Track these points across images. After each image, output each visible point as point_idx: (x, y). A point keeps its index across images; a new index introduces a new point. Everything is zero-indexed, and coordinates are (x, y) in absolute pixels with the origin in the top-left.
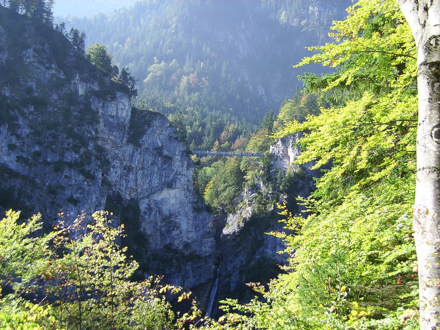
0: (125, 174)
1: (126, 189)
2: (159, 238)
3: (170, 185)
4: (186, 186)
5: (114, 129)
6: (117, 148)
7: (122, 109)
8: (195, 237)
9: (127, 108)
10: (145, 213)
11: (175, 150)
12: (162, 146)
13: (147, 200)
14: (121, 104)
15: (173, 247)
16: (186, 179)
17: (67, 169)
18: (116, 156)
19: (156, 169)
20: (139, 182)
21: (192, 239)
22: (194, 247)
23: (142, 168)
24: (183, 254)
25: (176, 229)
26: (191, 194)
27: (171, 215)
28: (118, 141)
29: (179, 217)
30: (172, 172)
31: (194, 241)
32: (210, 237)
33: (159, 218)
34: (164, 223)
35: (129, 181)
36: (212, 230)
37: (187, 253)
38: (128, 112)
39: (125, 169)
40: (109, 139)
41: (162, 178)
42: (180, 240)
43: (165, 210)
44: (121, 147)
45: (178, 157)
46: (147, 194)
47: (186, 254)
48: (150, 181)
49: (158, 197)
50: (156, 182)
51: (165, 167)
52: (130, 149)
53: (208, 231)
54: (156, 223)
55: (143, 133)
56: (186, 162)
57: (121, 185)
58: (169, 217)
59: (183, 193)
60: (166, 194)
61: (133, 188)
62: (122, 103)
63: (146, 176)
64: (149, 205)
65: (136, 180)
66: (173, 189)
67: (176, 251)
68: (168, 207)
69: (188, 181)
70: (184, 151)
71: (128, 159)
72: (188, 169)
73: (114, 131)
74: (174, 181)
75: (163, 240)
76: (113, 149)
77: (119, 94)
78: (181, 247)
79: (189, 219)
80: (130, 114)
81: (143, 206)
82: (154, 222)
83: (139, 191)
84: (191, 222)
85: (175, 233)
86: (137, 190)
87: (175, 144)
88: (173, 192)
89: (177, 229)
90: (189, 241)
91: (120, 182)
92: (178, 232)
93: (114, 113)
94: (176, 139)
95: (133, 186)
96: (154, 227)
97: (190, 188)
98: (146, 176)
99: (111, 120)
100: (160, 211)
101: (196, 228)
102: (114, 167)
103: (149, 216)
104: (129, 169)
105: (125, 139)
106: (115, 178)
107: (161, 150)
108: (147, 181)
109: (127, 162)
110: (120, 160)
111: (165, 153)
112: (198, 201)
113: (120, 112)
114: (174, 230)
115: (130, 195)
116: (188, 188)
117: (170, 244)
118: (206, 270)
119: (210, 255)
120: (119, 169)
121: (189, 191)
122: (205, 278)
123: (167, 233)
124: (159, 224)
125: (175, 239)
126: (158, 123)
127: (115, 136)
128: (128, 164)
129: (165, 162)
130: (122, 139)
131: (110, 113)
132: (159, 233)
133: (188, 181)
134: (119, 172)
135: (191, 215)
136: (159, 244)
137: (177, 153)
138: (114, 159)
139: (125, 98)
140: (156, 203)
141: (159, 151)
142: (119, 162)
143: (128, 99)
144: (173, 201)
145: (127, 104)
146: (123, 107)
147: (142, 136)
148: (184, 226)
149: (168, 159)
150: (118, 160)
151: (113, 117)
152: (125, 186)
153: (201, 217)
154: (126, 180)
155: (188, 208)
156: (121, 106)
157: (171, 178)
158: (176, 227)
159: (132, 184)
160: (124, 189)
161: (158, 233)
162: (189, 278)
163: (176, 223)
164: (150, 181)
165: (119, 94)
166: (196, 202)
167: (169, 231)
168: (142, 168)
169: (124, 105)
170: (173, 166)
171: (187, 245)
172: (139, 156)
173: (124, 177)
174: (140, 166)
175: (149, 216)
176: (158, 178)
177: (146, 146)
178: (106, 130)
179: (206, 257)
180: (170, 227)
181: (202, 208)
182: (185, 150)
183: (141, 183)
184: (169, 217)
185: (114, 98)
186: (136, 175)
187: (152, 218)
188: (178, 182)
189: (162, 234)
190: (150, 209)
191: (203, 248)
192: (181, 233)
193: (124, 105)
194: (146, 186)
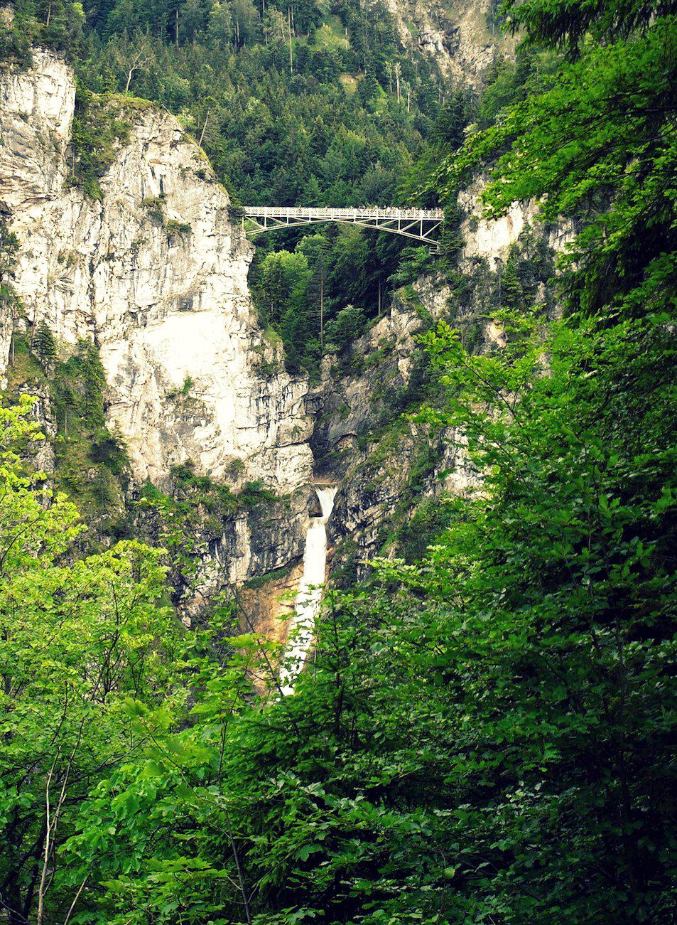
0: (62, 274)
2: (158, 447)
3: (185, 305)
4: (229, 306)
5: (28, 151)
6: (38, 201)
8: (256, 445)
10: (119, 380)
12: (162, 196)
13: (124, 344)
18: (35, 225)
20: (98, 298)
21: (248, 449)
22: (255, 471)
23: (110, 257)
24: (225, 490)
25: (203, 422)
26: (244, 327)
27: (189, 384)
28: (41, 184)
29: (210, 390)
30: (189, 265)
31: (255, 455)
32: (297, 444)
33: (155, 394)
34: (171, 408)
35: (72, 294)
36: (301, 424)
37: (235, 487)
39: (60, 260)
40: (15, 178)
41: (163, 282)
42: (216, 451)
46: (120, 327)
47: (231, 490)
48: (132, 291)
51: (172, 251)
52: (70, 204)
53: (292, 426)
54: (149, 406)
57: (50, 303)
58: (184, 393)
61: (83, 313)
63: (120, 278)
66: (193, 311)
67: (206, 485)
70: (222, 209)
75: (169, 453)
76: (26, 205)
77: (38, 55)
78: (218, 473)
79: (239, 396)
80: (71, 107)
81: (112, 362)
82: (142, 405)
83: (100, 320)
84: (245, 402)
85: (201, 434)
86: (93, 316)
87: (200, 190)
89: (209, 422)
90: (242, 455)
91: (46, 295)
92: (210, 430)
93: (27, 108)
94: (201, 175)
95: (83, 308)
96: (143, 418)
98: (120, 278)
99: (19, 125)
100: (158, 375)
101: (259, 419)
102: (30, 255)
105: (60, 179)
106: (34, 287)
107: (159, 208)
108: (124, 293)
109: (65, 240)
110: (47, 236)
111: (170, 213)
114: (197, 425)
117: (189, 464)
118: (287, 531)
119: (298, 493)
120: (42, 259)
121: (237, 318)
122: (284, 555)
123: (181, 434)
124: (158, 408)
125: (201, 448)
126: (150, 133)
127: (30, 170)
128: (70, 248)
129: (169, 239)
132: (158, 435)
133: (237, 290)
135: (247, 382)
136: (159, 464)
137: (203, 215)
138: (30, 234)
139: (57, 64)
142: (45, 240)
143: (65, 67)
146: (51, 89)
147: (107, 169)
151: (24, 117)
152: (62, 308)
153: (274, 388)
154: (64, 291)
155: (239, 364)
156: (45, 85)
157: (188, 284)
158: (204, 416)
159: (81, 301)
160: (60, 316)
161: (156, 435)
162: (243, 555)
163: (203, 406)
164: (132, 291)
165: (38, 55)
166: (257, 347)
167: (184, 430)
168: (110, 257)
170: (192, 249)
171: (235, 468)
172: (98, 222)
173: (59, 282)
174: (103, 251)
176: (154, 282)
177: (121, 197)
179: (288, 496)
180: (188, 418)
181: (275, 363)
182: (224, 205)
183: (107, 300)
184: (184, 393)
185: (25, 64)
186: (92, 275)
187: (137, 391)
189: (164, 436)
194: (120, 307)
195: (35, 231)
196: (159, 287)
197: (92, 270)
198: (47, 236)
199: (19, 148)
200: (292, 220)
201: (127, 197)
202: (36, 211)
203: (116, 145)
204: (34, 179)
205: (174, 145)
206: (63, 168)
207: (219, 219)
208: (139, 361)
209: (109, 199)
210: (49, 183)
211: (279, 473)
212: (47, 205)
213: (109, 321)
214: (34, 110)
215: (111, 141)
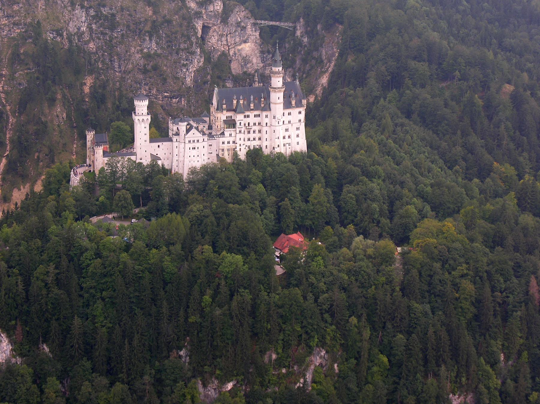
1: (221, 45)
3: (245, 42)
4: (255, 41)
8: (262, 66)
9: (220, 5)
10: (233, 56)
11: (247, 23)
13: (233, 49)
15: (248, 72)
16: (255, 37)
17: (181, 52)
19: (237, 34)
20: (228, 41)
23: (230, 34)
33: (240, 59)
38: (220, 6)
43: (244, 54)
45: (249, 26)
46: (233, 46)
48: (235, 39)
49: (239, 48)
50: (237, 40)
55: (229, 16)
59: (253, 44)
60: (243, 46)
64: (234, 52)
65: (227, 40)
68: (245, 52)
69: (256, 38)
72: (255, 31)
74: (247, 39)
80: (222, 7)
81: (231, 53)
83: (229, 44)
85: (248, 65)
88: (248, 44)
90: (259, 68)
92: (251, 64)
93: (212, 10)
94: (247, 17)
97: (257, 41)
99: (210, 13)
100: (240, 55)
102: (213, 36)
103: (235, 57)
104: (222, 36)
105: (219, 21)
107: (240, 23)
111: (243, 24)
112: (263, 47)
113: (216, 7)
114: (248, 64)
115: (224, 48)
116: (256, 42)
117: (246, 71)
124: (240, 61)
129: (242, 30)
133: (256, 38)
134: (217, 38)
135: (258, 55)
140: (239, 50)
141: (238, 24)
144: (247, 49)
145: (219, 3)
148: (254, 61)
149: (244, 28)
151: (211, 12)
156: (216, 4)
159: (225, 43)
161: (240, 66)
164: (235, 39)
167: (245, 65)
174: (229, 33)
175: (235, 57)
187: (236, 58)
188: (249, 39)
189: (242, 66)
190: (235, 54)
191: (266, 71)
192: (253, 64)
194: (233, 42)
196: (240, 39)
197: (227, 36)
202: (215, 27)
205: (243, 11)
208: (237, 52)
209: (229, 24)
210: (217, 22)
211: (266, 71)
213: (231, 44)
215: (230, 12)
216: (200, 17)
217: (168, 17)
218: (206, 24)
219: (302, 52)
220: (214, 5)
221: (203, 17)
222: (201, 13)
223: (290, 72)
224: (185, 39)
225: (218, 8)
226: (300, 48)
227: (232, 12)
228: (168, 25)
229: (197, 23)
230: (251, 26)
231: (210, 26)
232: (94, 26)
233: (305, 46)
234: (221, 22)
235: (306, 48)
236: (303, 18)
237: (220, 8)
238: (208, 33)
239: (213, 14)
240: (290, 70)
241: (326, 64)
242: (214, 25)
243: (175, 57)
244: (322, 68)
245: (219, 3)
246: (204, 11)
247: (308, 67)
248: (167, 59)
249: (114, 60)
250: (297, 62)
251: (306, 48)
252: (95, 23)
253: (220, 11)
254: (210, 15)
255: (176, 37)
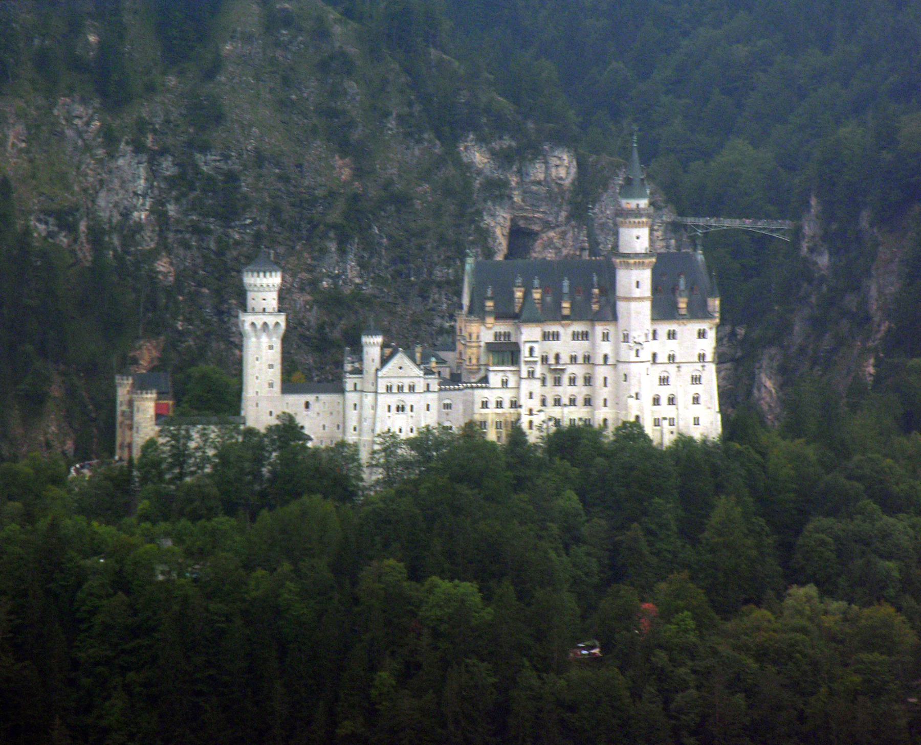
5: (540, 203)
6: (553, 228)
7: (557, 166)
9: (566, 163)
14: (555, 159)
17: (435, 290)
28: (550, 219)
32: (723, 363)
38: (568, 168)
40: (534, 217)
44: (558, 226)
56: (673, 242)
62: (555, 156)
71: (571, 243)
73: (539, 207)
80: (573, 170)
93: (541, 176)
99: (534, 188)
105: (563, 214)
113: (553, 171)
127: (543, 212)
128: (572, 252)
130: (558, 214)
131: (533, 178)
145: (565, 157)
146: (558, 162)
150: (551, 249)
151: (539, 183)
156: (554, 161)
169: (560, 158)
178: (527, 206)
193: (560, 158)
195: (548, 246)
198: (556, 248)
199: (535, 202)
200: (715, 227)
201: (608, 220)
202: (551, 234)
203: (600, 191)
204: (546, 217)
206: (564, 207)
207: (666, 228)
210: (556, 218)
212: (557, 230)
214: (545, 178)
216: (501, 197)
217: (399, 187)
218: (522, 223)
219: (813, 299)
220: (546, 163)
221: (510, 198)
222: (505, 184)
223: (772, 359)
224: (450, 254)
225: (562, 172)
226: (805, 285)
227: (605, 187)
228: (398, 211)
229: (493, 215)
230: (665, 232)
231: (536, 228)
232: (172, 209)
233: (823, 279)
234: (568, 219)
235: (825, 288)
236: (817, 196)
237: (568, 173)
238: (529, 253)
239: (543, 190)
240: (773, 351)
241: (879, 326)
242: (548, 226)
243: (416, 306)
244: (868, 338)
245: (565, 157)
246: (514, 180)
247: (827, 342)
248: (392, 313)
249: (229, 309)
250: (797, 328)
251: (825, 288)
252: (177, 200)
253: (567, 183)
254: (536, 193)
255: (421, 248)
